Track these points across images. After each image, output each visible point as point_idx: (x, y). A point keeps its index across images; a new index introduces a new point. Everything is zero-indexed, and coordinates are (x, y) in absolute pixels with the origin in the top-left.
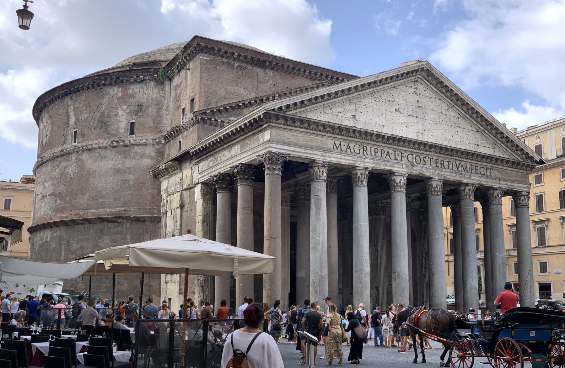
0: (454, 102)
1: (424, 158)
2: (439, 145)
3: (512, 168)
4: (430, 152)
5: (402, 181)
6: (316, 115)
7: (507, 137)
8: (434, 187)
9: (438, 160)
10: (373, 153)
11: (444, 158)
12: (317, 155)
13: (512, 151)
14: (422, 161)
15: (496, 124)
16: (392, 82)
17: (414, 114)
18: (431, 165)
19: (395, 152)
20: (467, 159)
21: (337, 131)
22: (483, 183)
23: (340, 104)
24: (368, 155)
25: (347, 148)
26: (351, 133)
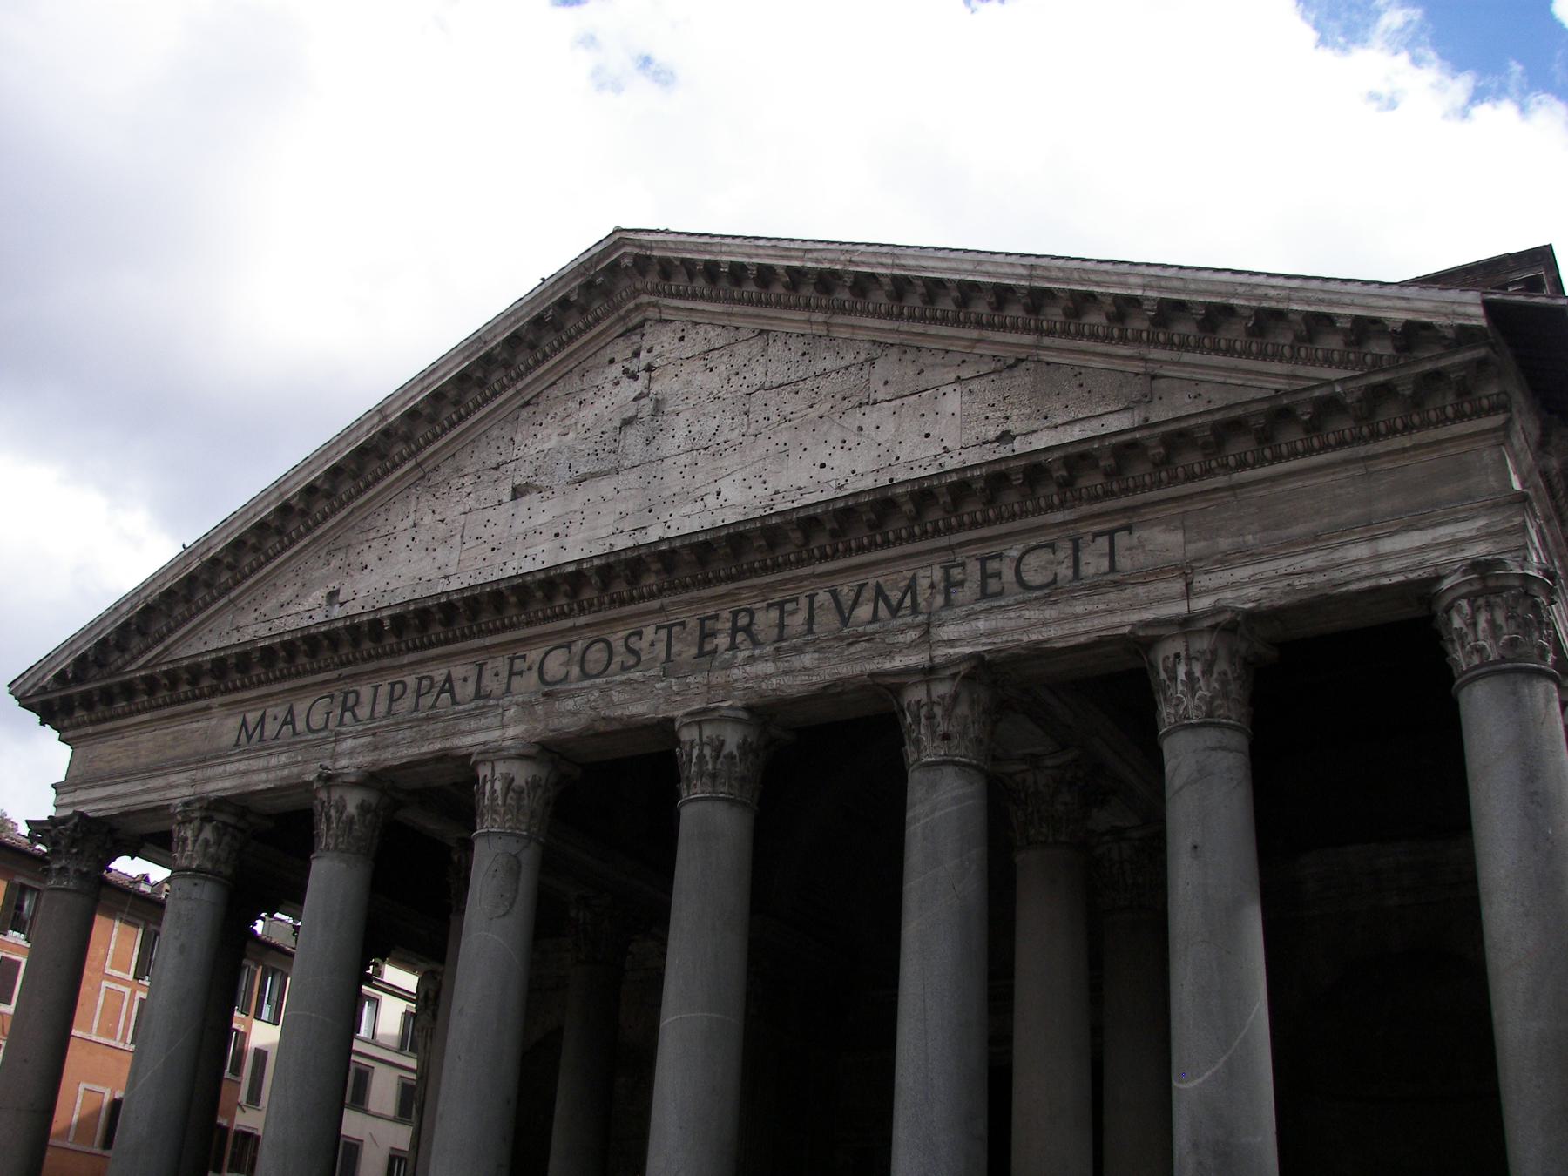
0: (819, 307)
1: (633, 639)
3: (1278, 458)
4: (642, 598)
5: (488, 786)
9: (716, 617)
10: (381, 708)
12: (177, 786)
13: (1277, 357)
14: (617, 659)
15: (1057, 280)
16: (495, 394)
17: (609, 462)
20: (886, 544)
22: (1034, 637)
23: (292, 574)
24: (359, 721)
25: (285, 723)
26: (282, 665)
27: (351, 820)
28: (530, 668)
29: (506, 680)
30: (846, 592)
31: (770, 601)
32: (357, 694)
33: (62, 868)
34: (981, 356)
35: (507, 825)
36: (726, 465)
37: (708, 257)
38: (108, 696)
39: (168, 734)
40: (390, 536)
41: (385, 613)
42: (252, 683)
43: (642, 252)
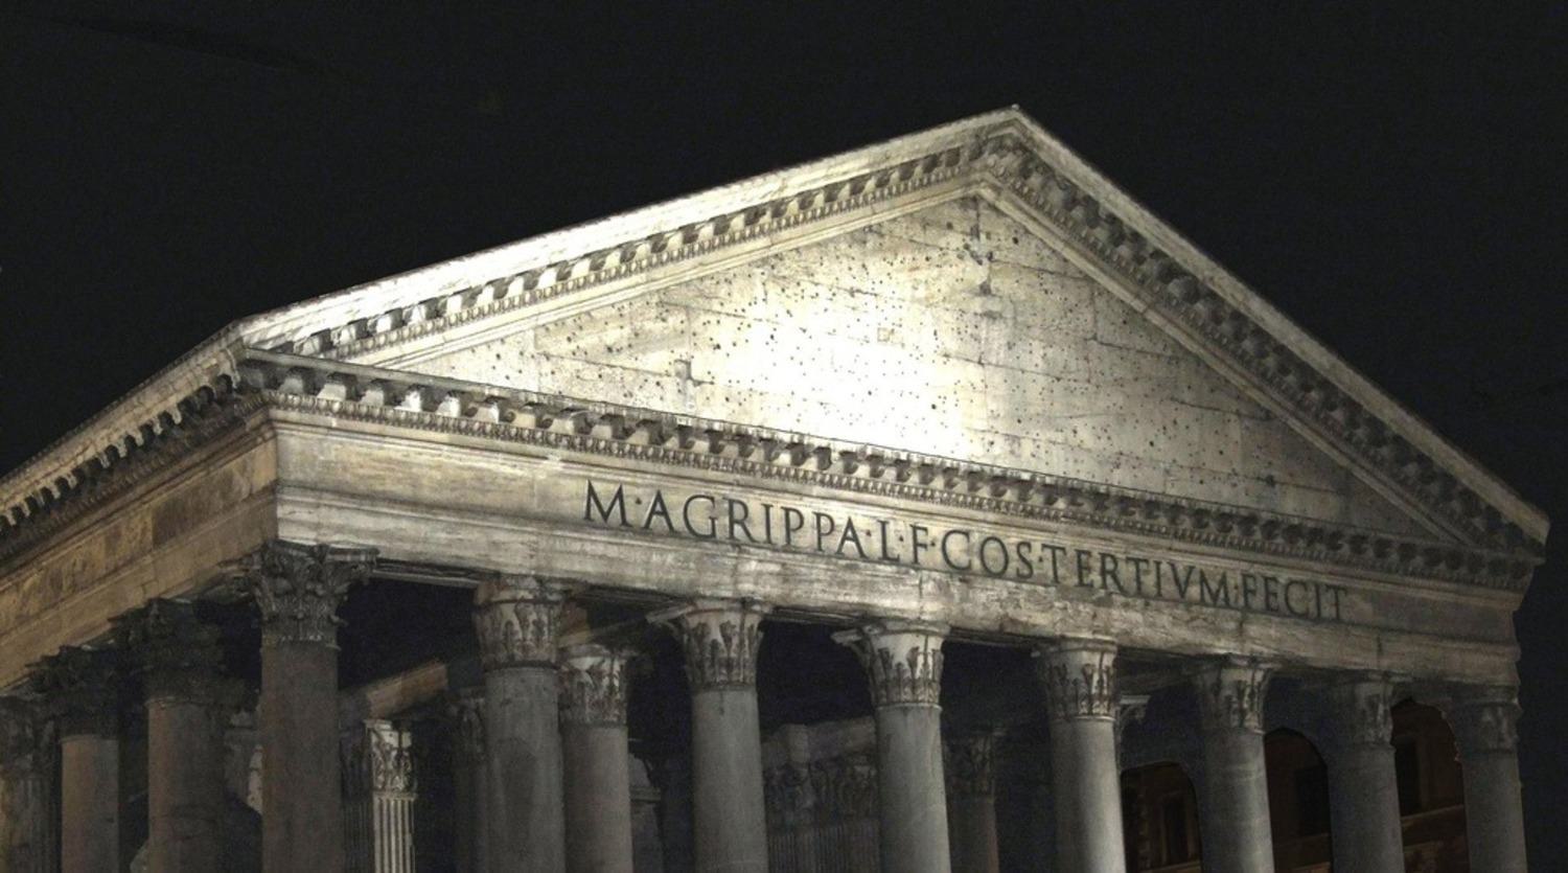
0: (1151, 287)
1: (1024, 550)
2: (1087, 485)
4: (1048, 517)
5: (920, 659)
6: (499, 364)
7: (1397, 439)
8: (1075, 682)
9: (1089, 553)
10: (778, 534)
11: (1117, 543)
15: (1340, 382)
16: (857, 205)
19: (884, 524)
20: (1222, 544)
21: (604, 431)
22: (1303, 654)
23: (614, 311)
25: (653, 512)
29: (911, 549)
31: (1130, 556)
32: (745, 508)
34: (1250, 398)
36: (1079, 404)
37: (1092, 194)
39: (462, 468)
41: (841, 447)
43: (1028, 145)
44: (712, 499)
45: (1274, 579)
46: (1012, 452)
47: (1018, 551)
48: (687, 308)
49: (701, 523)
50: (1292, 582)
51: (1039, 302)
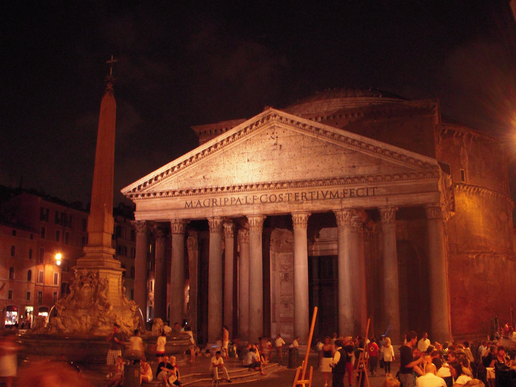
4: (283, 188)
5: (252, 222)
9: (298, 193)
10: (223, 203)
16: (241, 137)
18: (289, 200)
19: (246, 197)
22: (361, 205)
27: (218, 225)
28: (258, 199)
30: (325, 193)
33: (142, 231)
34: (349, 149)
35: (257, 229)
38: (149, 195)
40: (217, 165)
42: (188, 195)
44: (209, 199)
45: (353, 189)
46: (279, 176)
47: (279, 196)
48: (207, 166)
49: (207, 204)
50: (359, 189)
51: (289, 143)
